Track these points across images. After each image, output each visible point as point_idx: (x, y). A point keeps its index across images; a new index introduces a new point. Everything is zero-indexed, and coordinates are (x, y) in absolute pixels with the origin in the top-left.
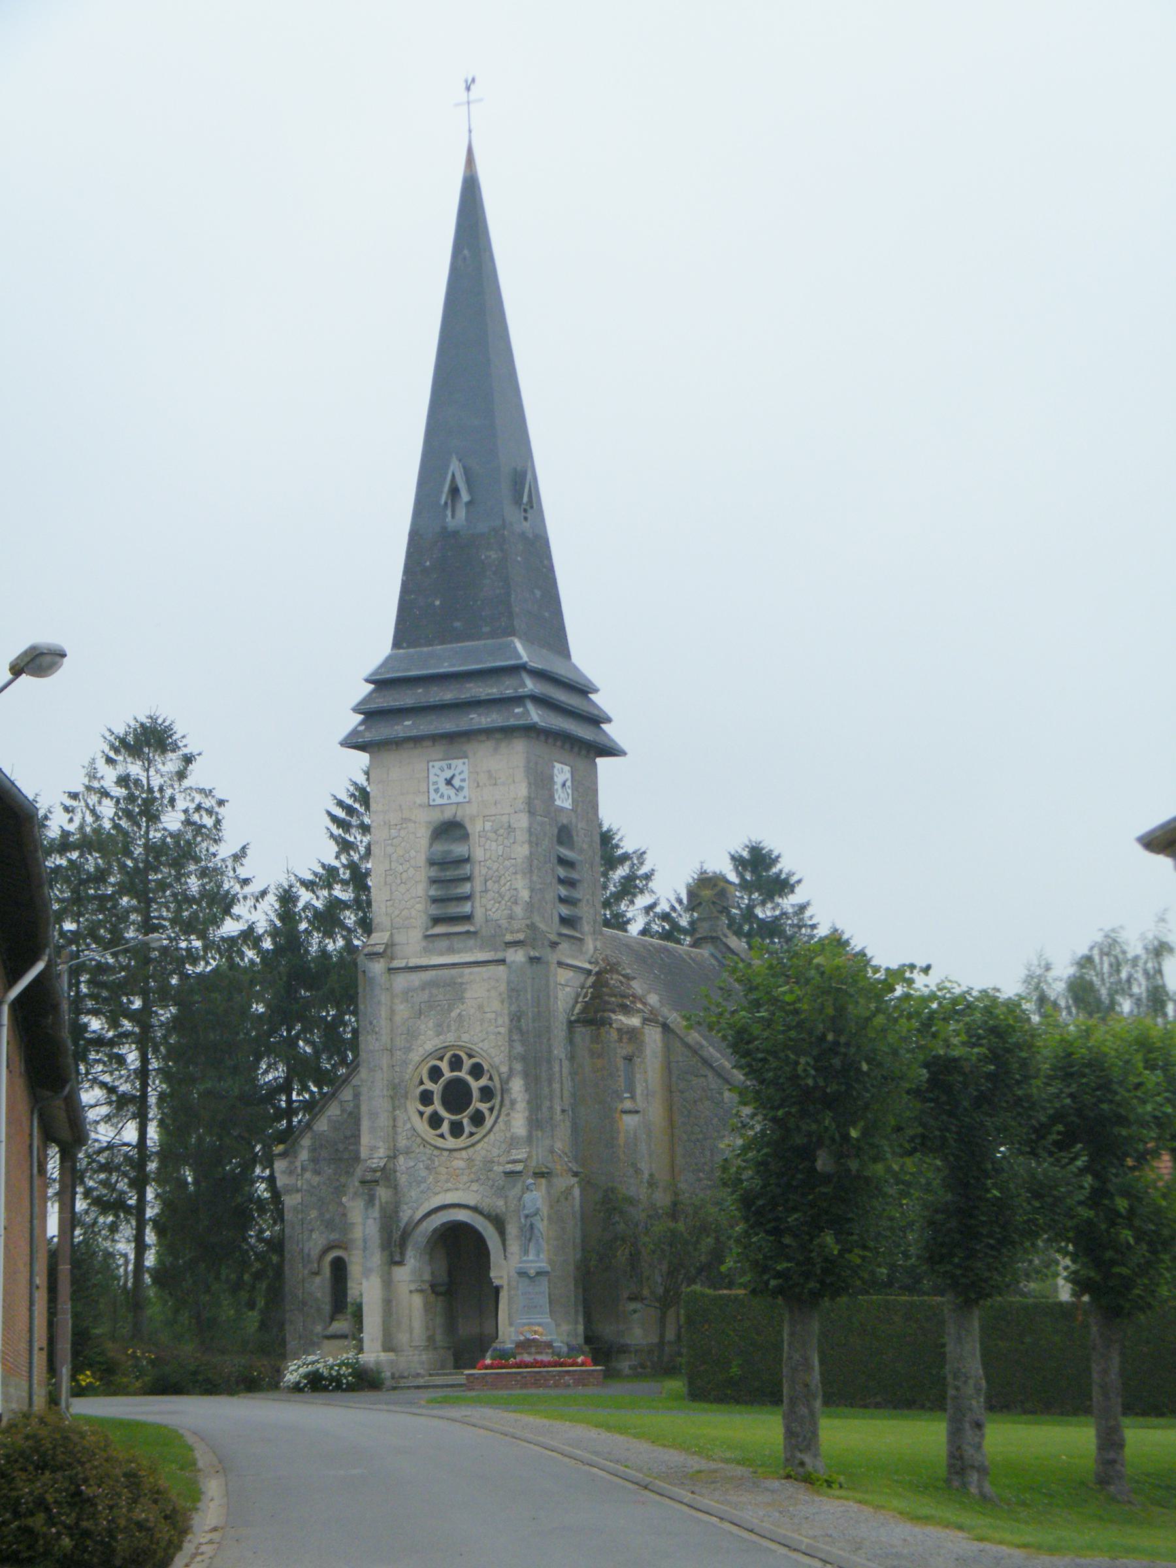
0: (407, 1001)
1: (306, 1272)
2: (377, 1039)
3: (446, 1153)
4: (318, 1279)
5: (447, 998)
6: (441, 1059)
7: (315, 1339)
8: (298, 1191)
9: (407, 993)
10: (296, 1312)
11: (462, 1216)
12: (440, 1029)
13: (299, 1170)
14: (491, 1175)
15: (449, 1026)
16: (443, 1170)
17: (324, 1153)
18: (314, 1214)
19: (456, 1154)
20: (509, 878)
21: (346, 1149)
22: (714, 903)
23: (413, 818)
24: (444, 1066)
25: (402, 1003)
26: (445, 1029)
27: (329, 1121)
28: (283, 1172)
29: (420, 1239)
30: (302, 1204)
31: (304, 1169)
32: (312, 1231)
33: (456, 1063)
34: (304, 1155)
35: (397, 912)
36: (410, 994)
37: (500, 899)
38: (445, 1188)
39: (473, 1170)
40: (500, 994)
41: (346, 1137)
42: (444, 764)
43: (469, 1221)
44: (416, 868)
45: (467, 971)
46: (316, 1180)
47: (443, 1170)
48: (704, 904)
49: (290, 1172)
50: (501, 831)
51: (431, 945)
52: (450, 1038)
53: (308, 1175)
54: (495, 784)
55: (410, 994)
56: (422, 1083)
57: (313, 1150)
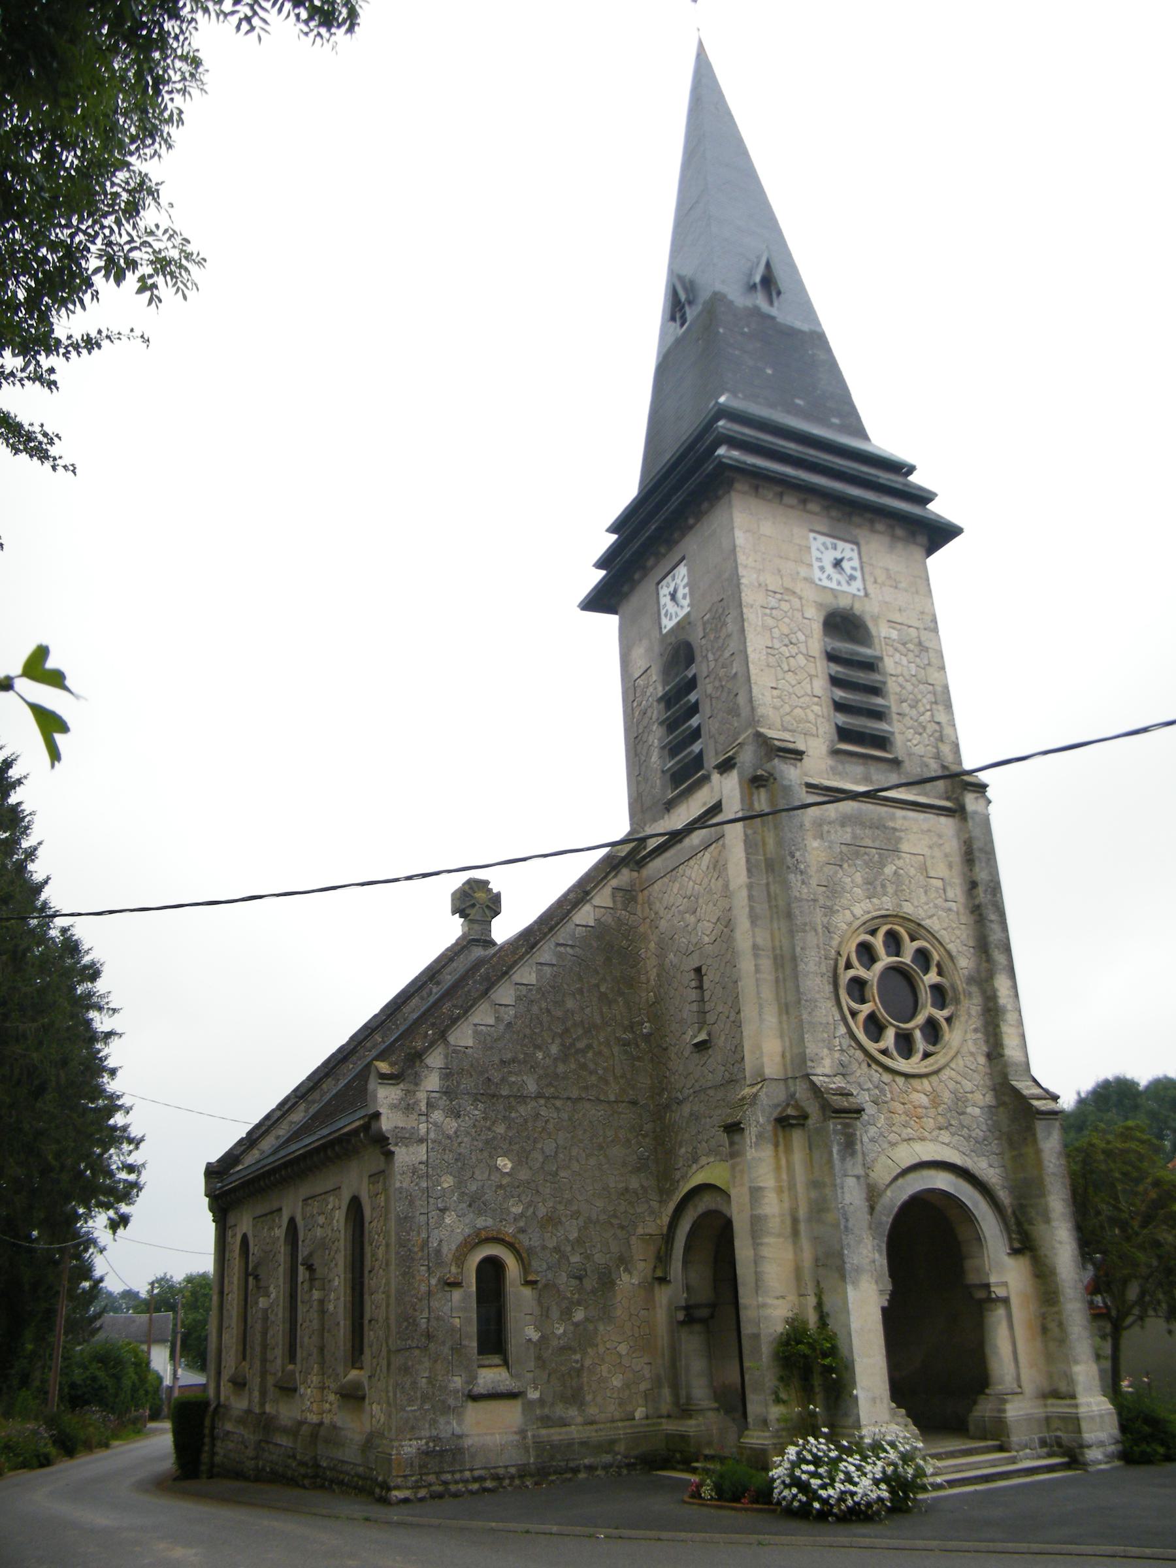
0: (822, 837)
1: (433, 1281)
2: (803, 882)
3: (900, 1080)
4: (457, 1295)
5: (877, 845)
6: (873, 932)
7: (451, 1401)
8: (421, 1141)
9: (820, 825)
10: (417, 1352)
11: (943, 1181)
12: (873, 887)
13: (424, 1109)
14: (966, 1120)
15: (883, 886)
16: (899, 1108)
17: (467, 1083)
18: (448, 1182)
19: (916, 1083)
20: (928, 707)
21: (503, 1079)
22: (488, 907)
23: (798, 591)
24: (878, 942)
25: (815, 838)
26: (879, 889)
27: (476, 1032)
28: (393, 1107)
29: (884, 1218)
30: (427, 1163)
31: (429, 1105)
32: (443, 1210)
33: (894, 942)
34: (432, 1082)
35: (787, 708)
36: (826, 828)
37: (921, 731)
38: (904, 1136)
39: (940, 1109)
40: (946, 856)
41: (503, 1062)
42: (829, 541)
43: (951, 1191)
44: (808, 656)
45: (899, 813)
46: (451, 1125)
47: (899, 1108)
48: (478, 906)
49: (408, 1108)
50: (910, 646)
51: (840, 767)
52: (887, 904)
53: (437, 1116)
54: (896, 587)
55: (826, 828)
56: (849, 966)
57: (447, 1074)
